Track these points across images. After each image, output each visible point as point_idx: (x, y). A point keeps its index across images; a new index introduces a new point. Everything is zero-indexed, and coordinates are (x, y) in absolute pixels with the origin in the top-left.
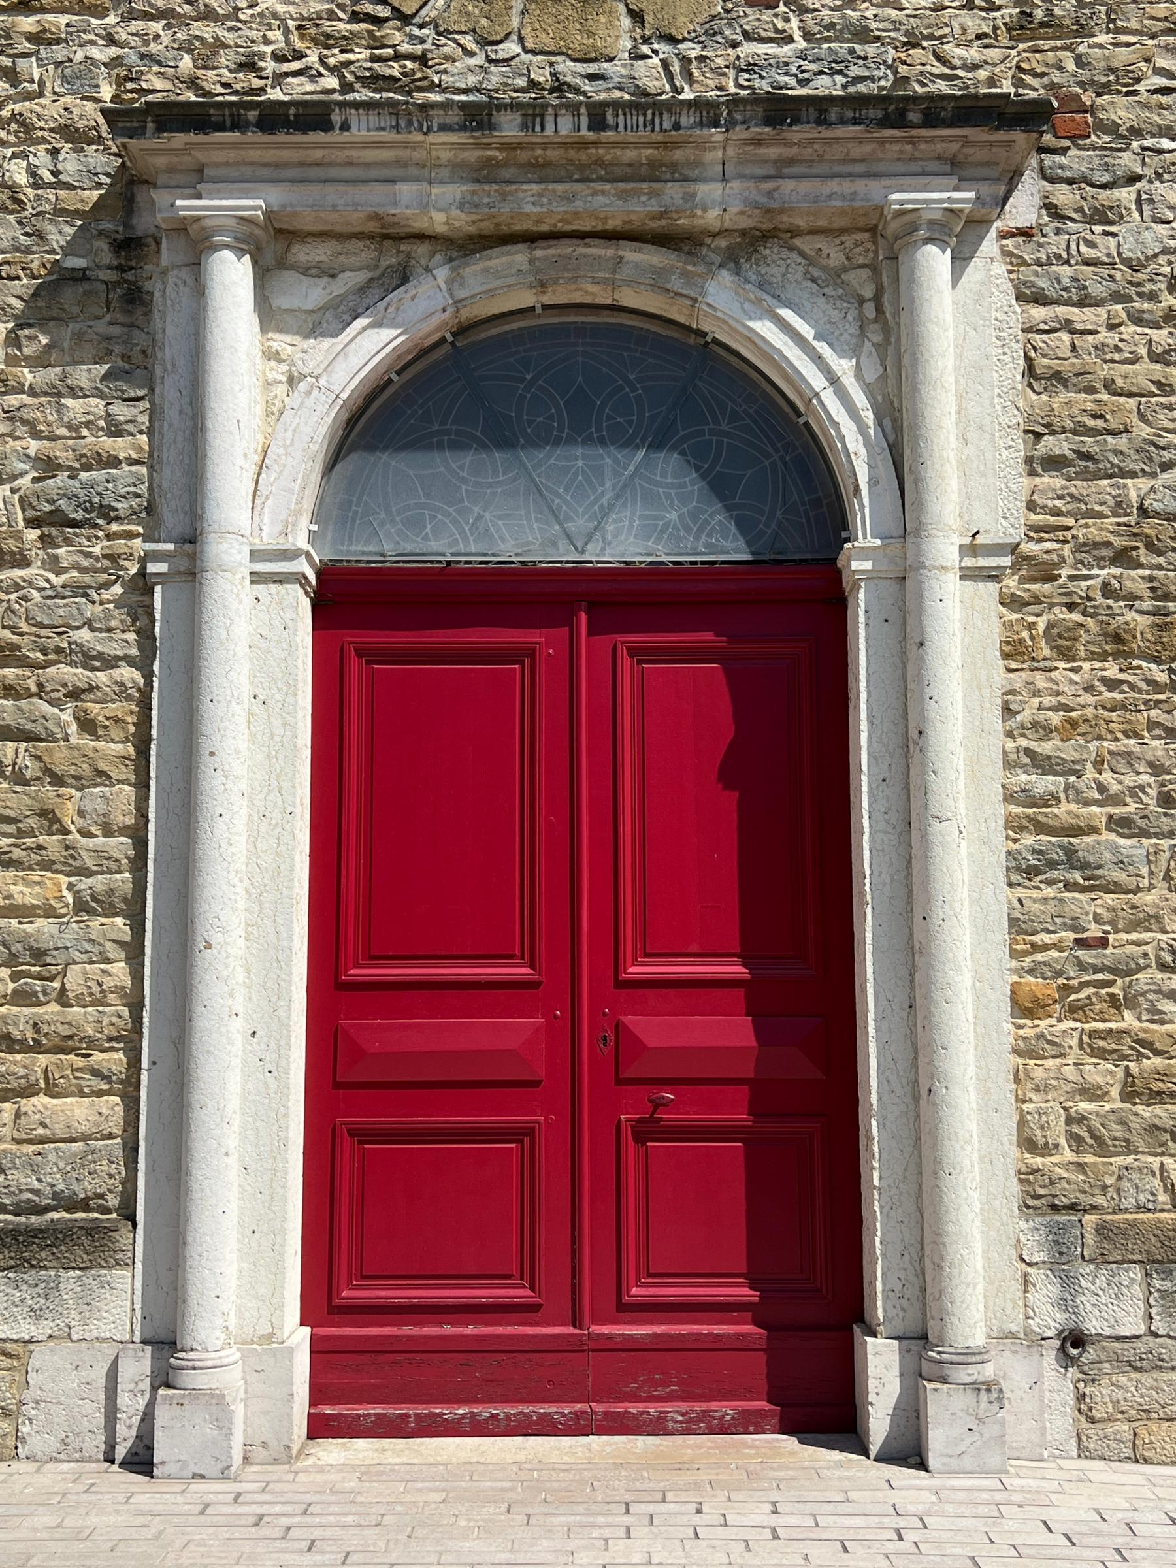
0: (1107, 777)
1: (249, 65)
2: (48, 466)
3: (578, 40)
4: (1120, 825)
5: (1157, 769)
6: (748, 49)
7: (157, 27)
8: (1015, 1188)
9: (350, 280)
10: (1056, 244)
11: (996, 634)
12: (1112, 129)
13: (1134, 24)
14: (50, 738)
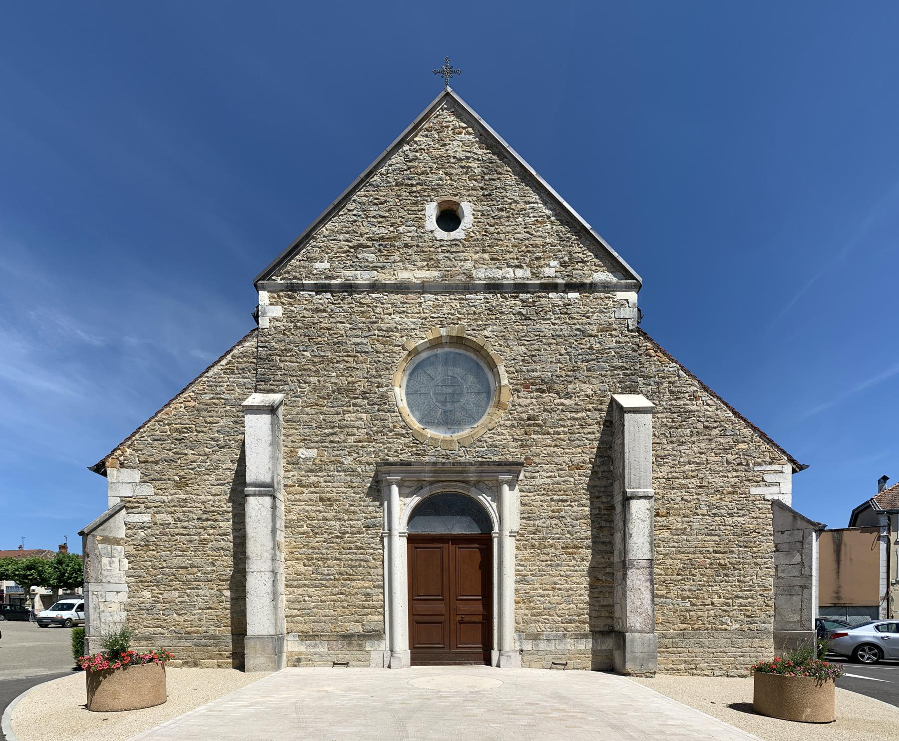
0: (530, 567)
1: (396, 451)
2: (366, 518)
3: (450, 448)
4: (532, 575)
5: (538, 566)
6: (477, 449)
7: (381, 445)
8: (514, 629)
9: (414, 488)
10: (526, 482)
11: (514, 545)
12: (535, 463)
13: (539, 445)
14: (368, 561)
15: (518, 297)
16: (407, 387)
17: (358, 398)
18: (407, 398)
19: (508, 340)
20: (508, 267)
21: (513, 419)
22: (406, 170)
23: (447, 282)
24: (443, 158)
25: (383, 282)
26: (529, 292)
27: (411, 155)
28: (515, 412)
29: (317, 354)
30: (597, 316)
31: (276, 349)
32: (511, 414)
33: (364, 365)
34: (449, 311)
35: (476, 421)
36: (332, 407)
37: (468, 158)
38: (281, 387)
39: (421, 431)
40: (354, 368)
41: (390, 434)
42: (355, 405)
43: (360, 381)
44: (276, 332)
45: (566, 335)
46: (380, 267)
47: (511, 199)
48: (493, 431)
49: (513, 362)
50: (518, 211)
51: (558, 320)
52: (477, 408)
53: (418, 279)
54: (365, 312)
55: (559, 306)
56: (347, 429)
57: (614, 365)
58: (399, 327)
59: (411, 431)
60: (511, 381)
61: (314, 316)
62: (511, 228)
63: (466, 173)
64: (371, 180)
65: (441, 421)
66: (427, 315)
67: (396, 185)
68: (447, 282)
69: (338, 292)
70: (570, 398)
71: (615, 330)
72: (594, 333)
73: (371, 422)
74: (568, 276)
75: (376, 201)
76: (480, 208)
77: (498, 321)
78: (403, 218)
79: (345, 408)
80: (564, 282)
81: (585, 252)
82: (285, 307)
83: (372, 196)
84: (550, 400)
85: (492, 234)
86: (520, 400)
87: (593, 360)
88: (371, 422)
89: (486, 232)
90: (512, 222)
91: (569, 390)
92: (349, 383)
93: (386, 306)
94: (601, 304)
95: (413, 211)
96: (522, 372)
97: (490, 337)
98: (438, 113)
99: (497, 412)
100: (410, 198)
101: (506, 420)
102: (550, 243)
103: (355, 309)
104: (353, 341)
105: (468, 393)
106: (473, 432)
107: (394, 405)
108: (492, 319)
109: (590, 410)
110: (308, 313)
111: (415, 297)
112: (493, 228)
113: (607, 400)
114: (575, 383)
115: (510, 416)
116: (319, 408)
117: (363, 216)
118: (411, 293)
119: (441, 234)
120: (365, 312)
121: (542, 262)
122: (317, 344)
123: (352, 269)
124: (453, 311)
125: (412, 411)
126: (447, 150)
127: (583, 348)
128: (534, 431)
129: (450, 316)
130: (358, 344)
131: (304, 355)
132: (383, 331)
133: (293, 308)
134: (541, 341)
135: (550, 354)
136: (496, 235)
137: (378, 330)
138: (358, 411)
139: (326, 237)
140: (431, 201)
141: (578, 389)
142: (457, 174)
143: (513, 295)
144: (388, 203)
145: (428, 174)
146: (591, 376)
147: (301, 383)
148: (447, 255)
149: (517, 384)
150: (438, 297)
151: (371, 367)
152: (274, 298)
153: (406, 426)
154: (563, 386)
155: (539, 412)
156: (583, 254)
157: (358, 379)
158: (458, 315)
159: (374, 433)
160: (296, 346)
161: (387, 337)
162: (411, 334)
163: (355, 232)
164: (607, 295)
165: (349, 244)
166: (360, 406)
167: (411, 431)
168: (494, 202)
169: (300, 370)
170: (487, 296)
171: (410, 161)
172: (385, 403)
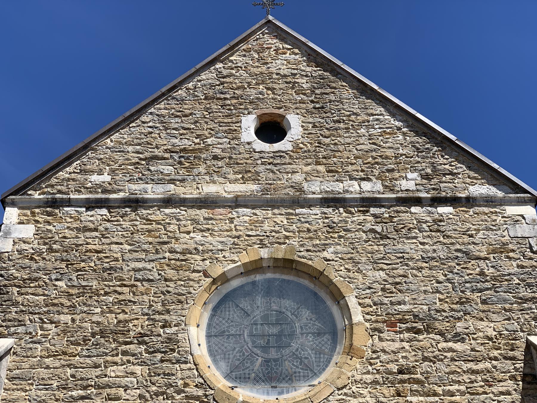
15: (368, 211)
16: (209, 326)
17: (131, 343)
18: (208, 342)
19: (359, 263)
20: (351, 179)
21: (375, 371)
22: (219, 85)
23: (269, 196)
24: (264, 75)
25: (182, 196)
26: (383, 206)
27: (225, 72)
28: (378, 361)
29: (75, 283)
30: (484, 234)
31: (16, 278)
32: (371, 364)
33: (145, 297)
34: (273, 228)
35: (316, 375)
36: (89, 356)
37: (295, 75)
38: (13, 329)
39: (229, 391)
40: (130, 301)
41: (178, 397)
42: (125, 353)
43: (137, 319)
44: (21, 256)
45: (442, 257)
46: (179, 181)
47: (349, 111)
48: (345, 390)
49: (368, 291)
50: (360, 122)
51: (429, 239)
52: (318, 356)
53: (229, 193)
54: (153, 231)
55: (426, 222)
56: (108, 390)
57: (520, 295)
58: (200, 248)
59: (213, 392)
60: (368, 317)
61: (79, 235)
62: (352, 139)
63: (293, 88)
64: (174, 94)
65: (261, 375)
66: (241, 233)
67: (206, 99)
68: (269, 196)
69: (119, 207)
70: (463, 340)
71: (513, 251)
72: (483, 255)
73: (148, 378)
74: (434, 189)
75: (179, 114)
76: (311, 120)
77: (342, 240)
78: (212, 130)
79: (109, 358)
80: (429, 196)
81: (452, 164)
82: (39, 225)
83: (174, 109)
84: (431, 344)
85: (328, 145)
86: (384, 344)
87: (488, 289)
88: (148, 378)
89: (319, 143)
90: (352, 133)
91: (459, 330)
92: (119, 322)
93: (184, 222)
94: (486, 221)
95: (226, 123)
96: (382, 304)
97: (333, 260)
98: (258, 37)
99: (349, 362)
100: (222, 111)
101: (365, 373)
102: (405, 155)
103: (139, 227)
104: (133, 266)
105: (302, 334)
106: (312, 393)
107: (186, 352)
108: (335, 238)
109: (496, 359)
110: (71, 232)
111: (224, 212)
112: (329, 139)
113: (521, 344)
114: (466, 320)
115: (370, 368)
116: (68, 358)
117: (161, 128)
118: (219, 207)
119: (260, 145)
120: (153, 231)
121: (396, 175)
122: (78, 271)
123: (140, 182)
124: (277, 228)
125: (215, 361)
126: (269, 68)
127: (471, 274)
128: (411, 391)
129: (273, 234)
130: (139, 270)
131: (56, 286)
132: (177, 253)
133: (50, 227)
134: (407, 265)
135: (422, 281)
136: (332, 146)
137: (170, 252)
138: (129, 361)
139: (110, 149)
140: (249, 114)
141: (472, 328)
142: (281, 89)
143: (361, 209)
144: (194, 116)
145: (246, 89)
146: (489, 311)
147: (46, 323)
148: (269, 167)
149: (377, 321)
150: (257, 211)
151: (156, 299)
152: (27, 216)
153: (205, 384)
154: (448, 324)
155: (416, 361)
156: (451, 166)
157: (134, 316)
158: (285, 233)
159: (151, 396)
160: (46, 275)
161: (182, 260)
162: (217, 256)
163: (148, 144)
164: (492, 210)
165: (141, 156)
166: (133, 355)
167: (213, 392)
168: (329, 115)
169: (47, 305)
170: (325, 210)
171: (223, 78)
172: (173, 350)
